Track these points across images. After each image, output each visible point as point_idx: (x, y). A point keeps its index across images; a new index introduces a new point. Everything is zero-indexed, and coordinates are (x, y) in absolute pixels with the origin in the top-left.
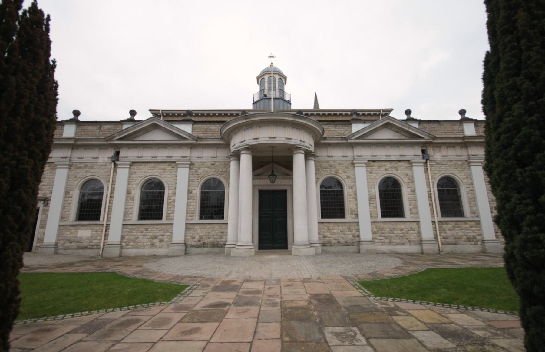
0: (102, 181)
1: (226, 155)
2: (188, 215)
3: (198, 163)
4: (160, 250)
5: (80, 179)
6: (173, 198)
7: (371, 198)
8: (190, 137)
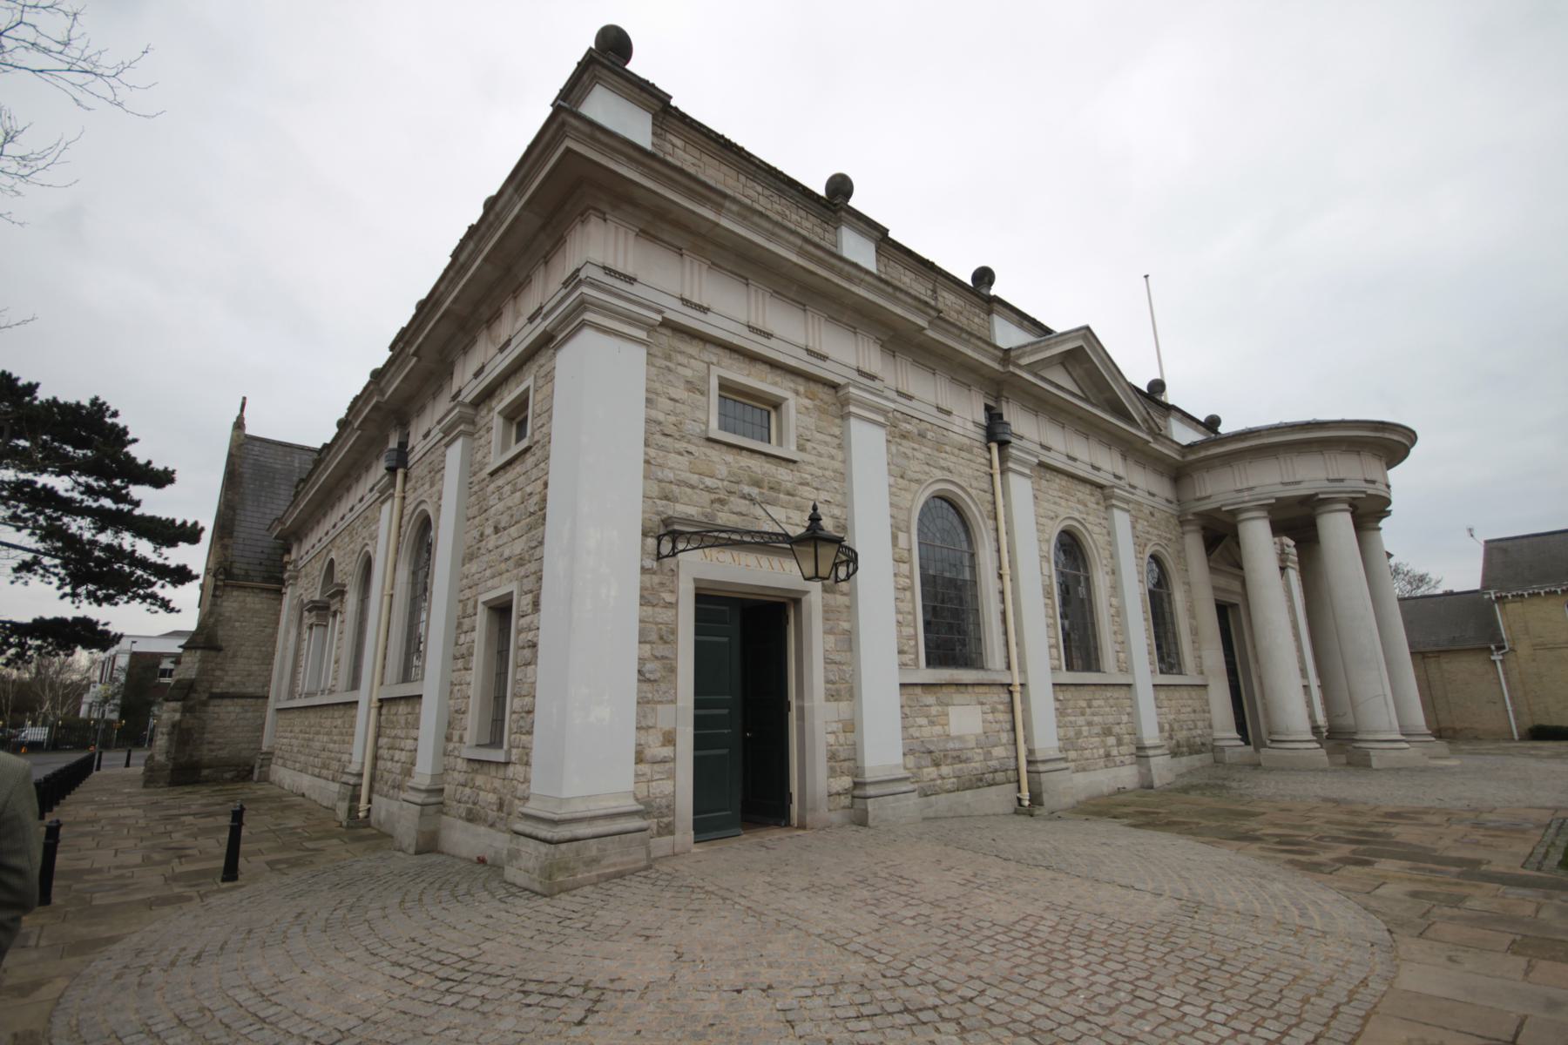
8: (1145, 421)
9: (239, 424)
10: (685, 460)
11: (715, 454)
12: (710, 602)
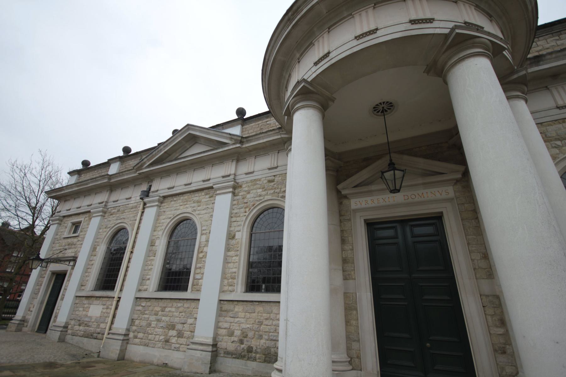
2: (226, 282)
3: (247, 183)
5: (109, 229)
6: (205, 249)
8: (231, 139)
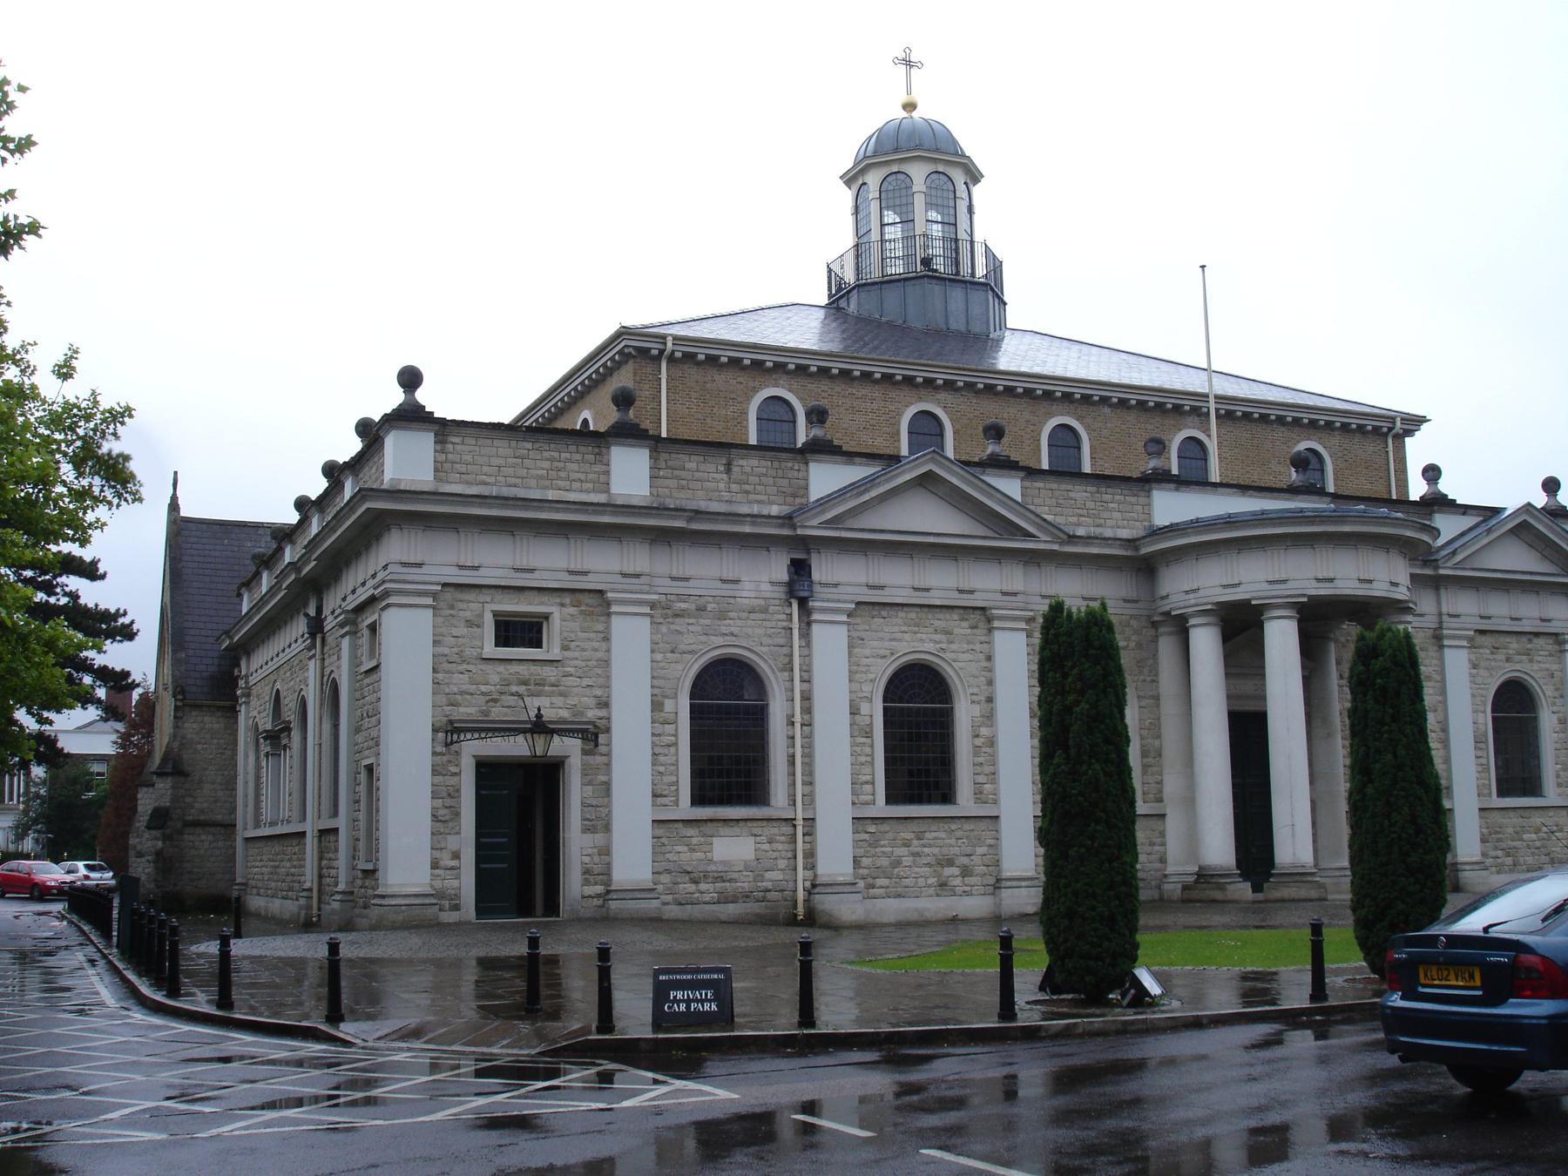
0: (764, 667)
1: (1123, 593)
4: (967, 901)
6: (984, 731)
7: (1479, 741)
9: (174, 506)
10: (465, 677)
11: (488, 668)
12: (487, 770)
